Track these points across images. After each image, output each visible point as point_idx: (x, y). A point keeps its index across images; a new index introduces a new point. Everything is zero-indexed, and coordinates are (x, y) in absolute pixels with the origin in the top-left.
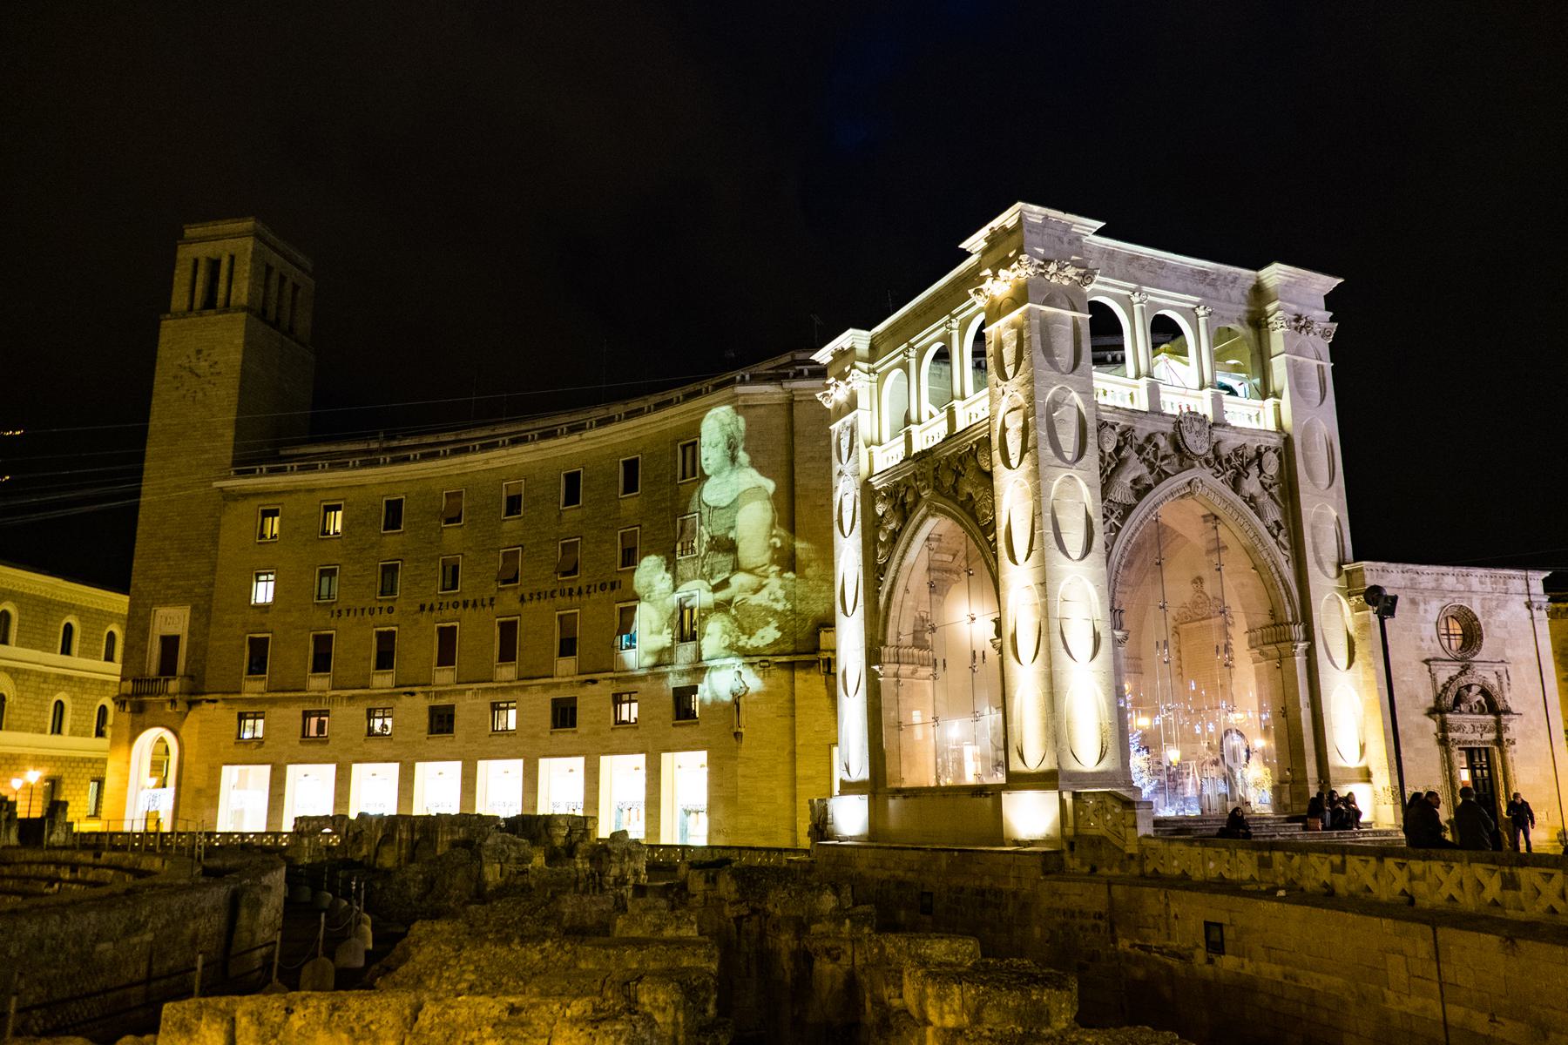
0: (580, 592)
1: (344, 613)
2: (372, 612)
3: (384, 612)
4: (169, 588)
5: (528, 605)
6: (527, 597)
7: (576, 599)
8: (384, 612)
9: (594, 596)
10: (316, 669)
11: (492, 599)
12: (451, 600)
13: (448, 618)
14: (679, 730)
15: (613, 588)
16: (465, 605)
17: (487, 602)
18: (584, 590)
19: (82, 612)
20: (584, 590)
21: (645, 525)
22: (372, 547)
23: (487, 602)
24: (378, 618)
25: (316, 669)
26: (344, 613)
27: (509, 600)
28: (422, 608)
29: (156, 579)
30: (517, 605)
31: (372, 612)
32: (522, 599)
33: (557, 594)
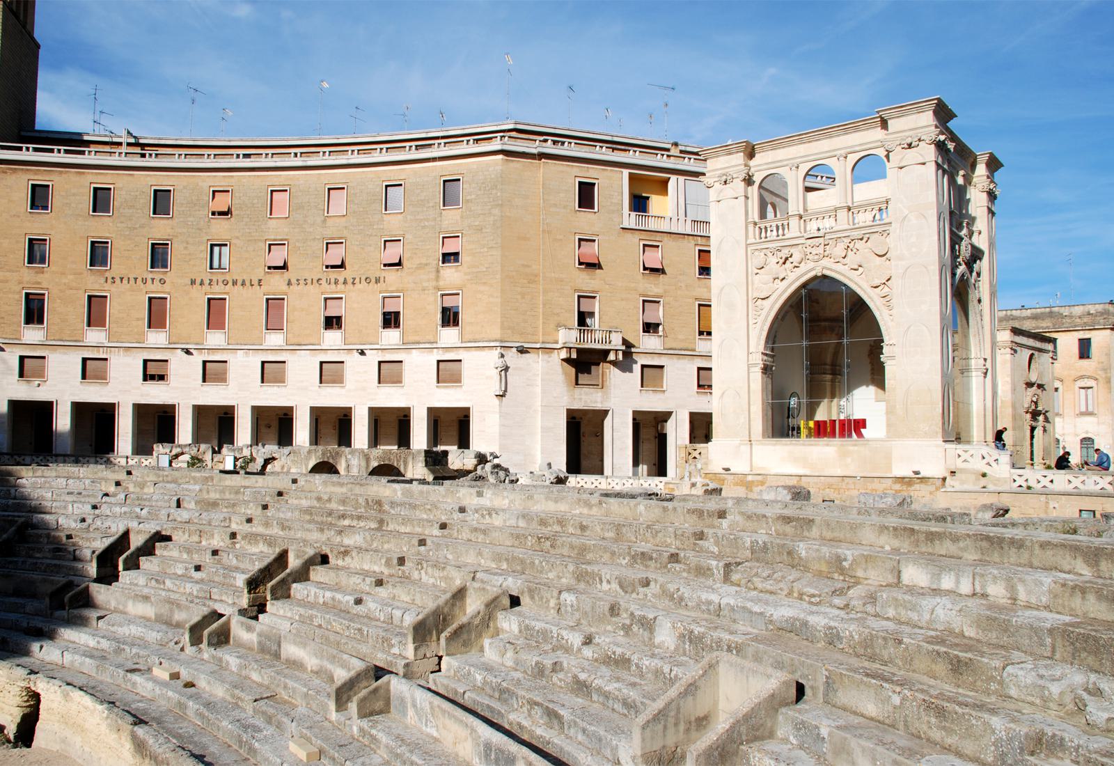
0: (345, 282)
1: (118, 280)
2: (145, 281)
5: (294, 288)
6: (294, 281)
7: (341, 287)
9: (358, 286)
10: (29, 320)
11: (260, 280)
12: (221, 278)
13: (217, 291)
15: (378, 280)
16: (235, 283)
17: (255, 282)
21: (409, 237)
22: (142, 226)
23: (255, 282)
24: (150, 286)
25: (29, 320)
26: (118, 280)
27: (276, 283)
28: (193, 282)
30: (284, 287)
31: (145, 281)
32: (289, 283)
33: (323, 282)
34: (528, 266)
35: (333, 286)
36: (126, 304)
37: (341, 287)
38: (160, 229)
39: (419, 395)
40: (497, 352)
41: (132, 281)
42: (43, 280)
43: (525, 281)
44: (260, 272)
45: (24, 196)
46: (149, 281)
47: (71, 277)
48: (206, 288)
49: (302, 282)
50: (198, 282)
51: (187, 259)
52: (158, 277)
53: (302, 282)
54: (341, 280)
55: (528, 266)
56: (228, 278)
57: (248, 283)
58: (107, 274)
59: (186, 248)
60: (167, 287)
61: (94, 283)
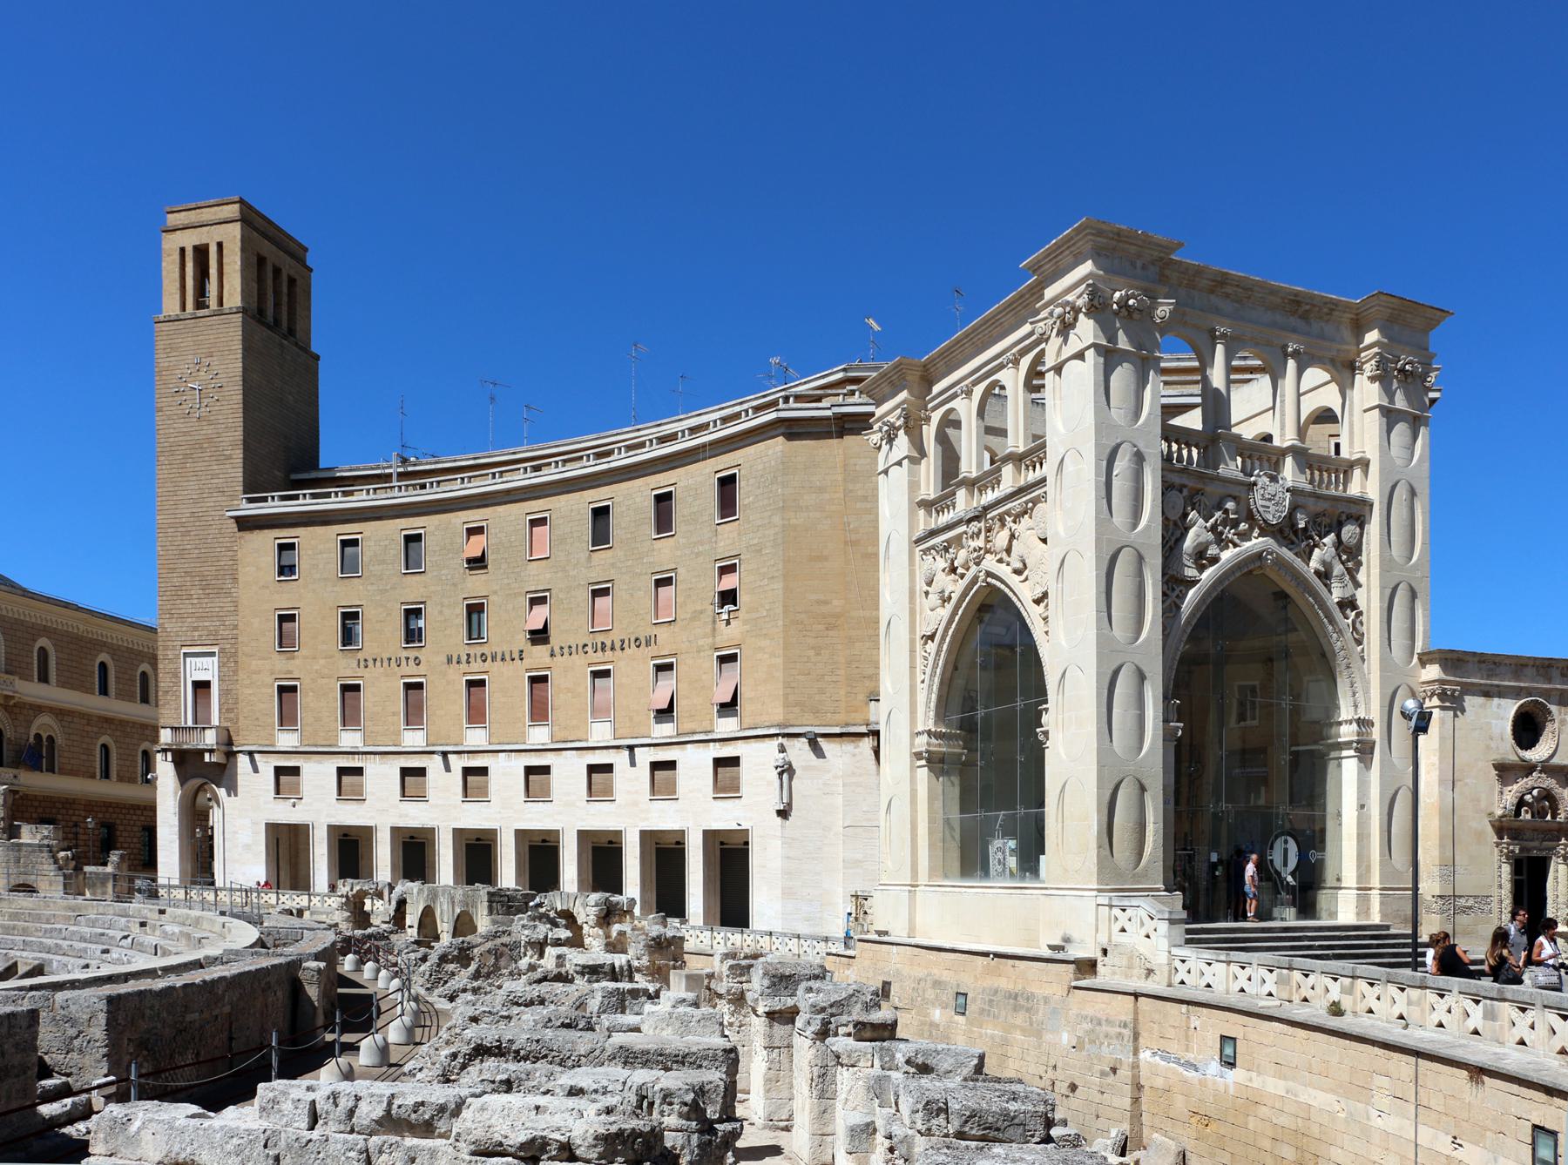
1: (370, 663)
3: (411, 662)
4: (196, 629)
5: (558, 658)
6: (557, 650)
7: (609, 653)
8: (411, 662)
13: (476, 670)
14: (720, 803)
16: (494, 659)
18: (618, 645)
19: (114, 650)
20: (618, 645)
22: (393, 588)
26: (370, 663)
27: (538, 656)
28: (449, 660)
29: (181, 618)
30: (547, 660)
34: (826, 603)
35: (600, 653)
36: (381, 693)
37: (609, 653)
38: (413, 589)
39: (694, 813)
40: (776, 742)
41: (386, 663)
42: (295, 668)
43: (821, 627)
44: (522, 640)
45: (270, 560)
46: (404, 662)
47: (322, 662)
48: (464, 666)
49: (566, 651)
50: (455, 659)
51: (445, 626)
52: (412, 654)
53: (566, 651)
54: (609, 644)
55: (826, 603)
56: (486, 650)
57: (508, 657)
58: (360, 655)
59: (441, 612)
60: (422, 669)
61: (347, 668)
